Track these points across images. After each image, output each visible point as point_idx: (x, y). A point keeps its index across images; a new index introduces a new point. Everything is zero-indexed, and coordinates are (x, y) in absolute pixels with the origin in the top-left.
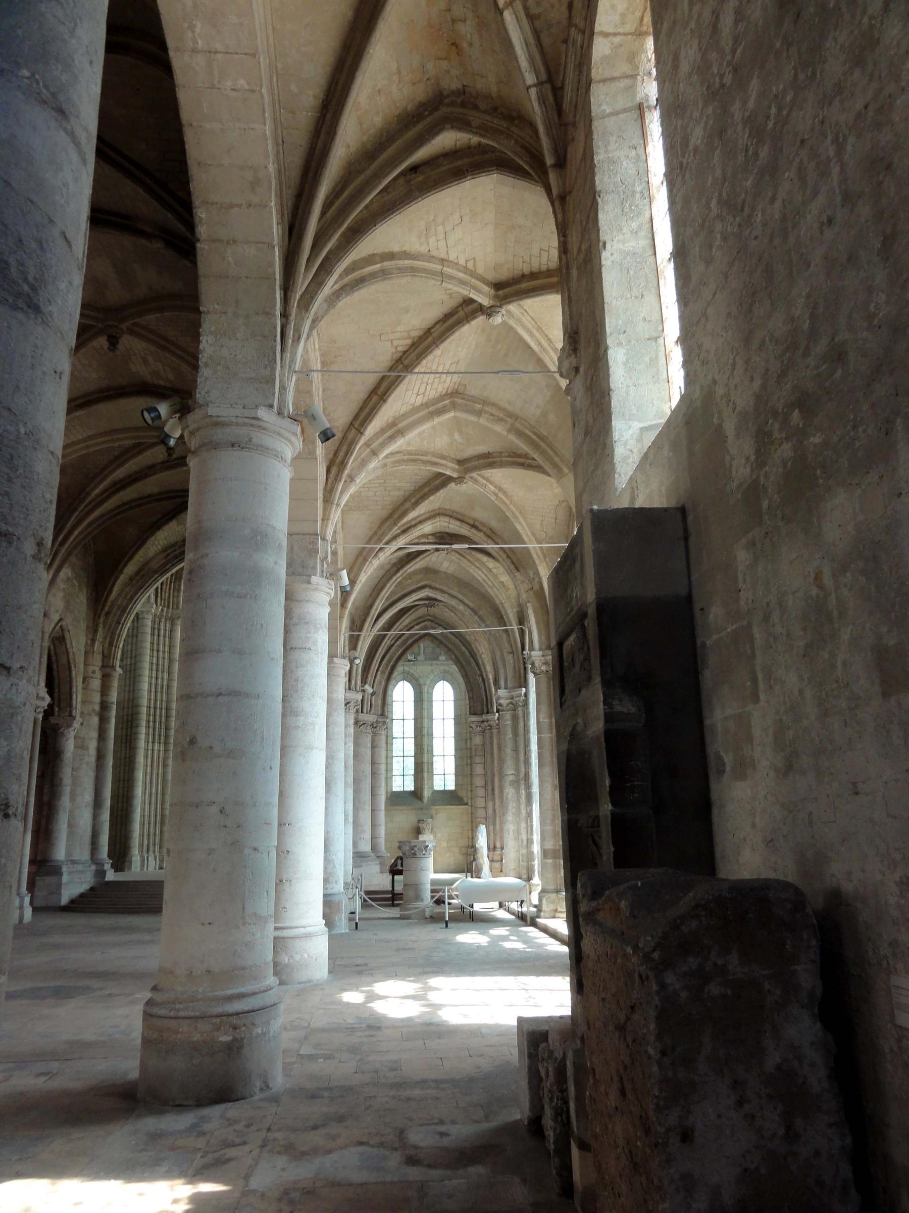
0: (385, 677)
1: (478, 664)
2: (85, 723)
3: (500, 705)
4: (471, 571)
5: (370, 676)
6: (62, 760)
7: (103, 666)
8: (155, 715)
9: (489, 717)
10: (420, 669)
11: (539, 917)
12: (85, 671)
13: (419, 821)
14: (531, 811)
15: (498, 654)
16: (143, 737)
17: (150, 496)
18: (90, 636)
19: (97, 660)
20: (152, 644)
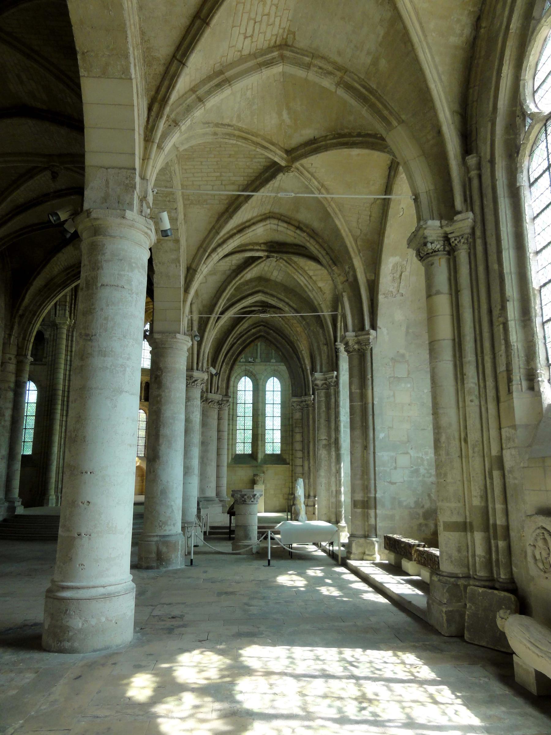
1: (298, 358)
3: (317, 385)
4: (295, 277)
9: (307, 398)
10: (258, 368)
11: (349, 559)
13: (255, 475)
14: (340, 468)
15: (315, 345)
16: (59, 411)
19: (13, 350)
20: (67, 346)
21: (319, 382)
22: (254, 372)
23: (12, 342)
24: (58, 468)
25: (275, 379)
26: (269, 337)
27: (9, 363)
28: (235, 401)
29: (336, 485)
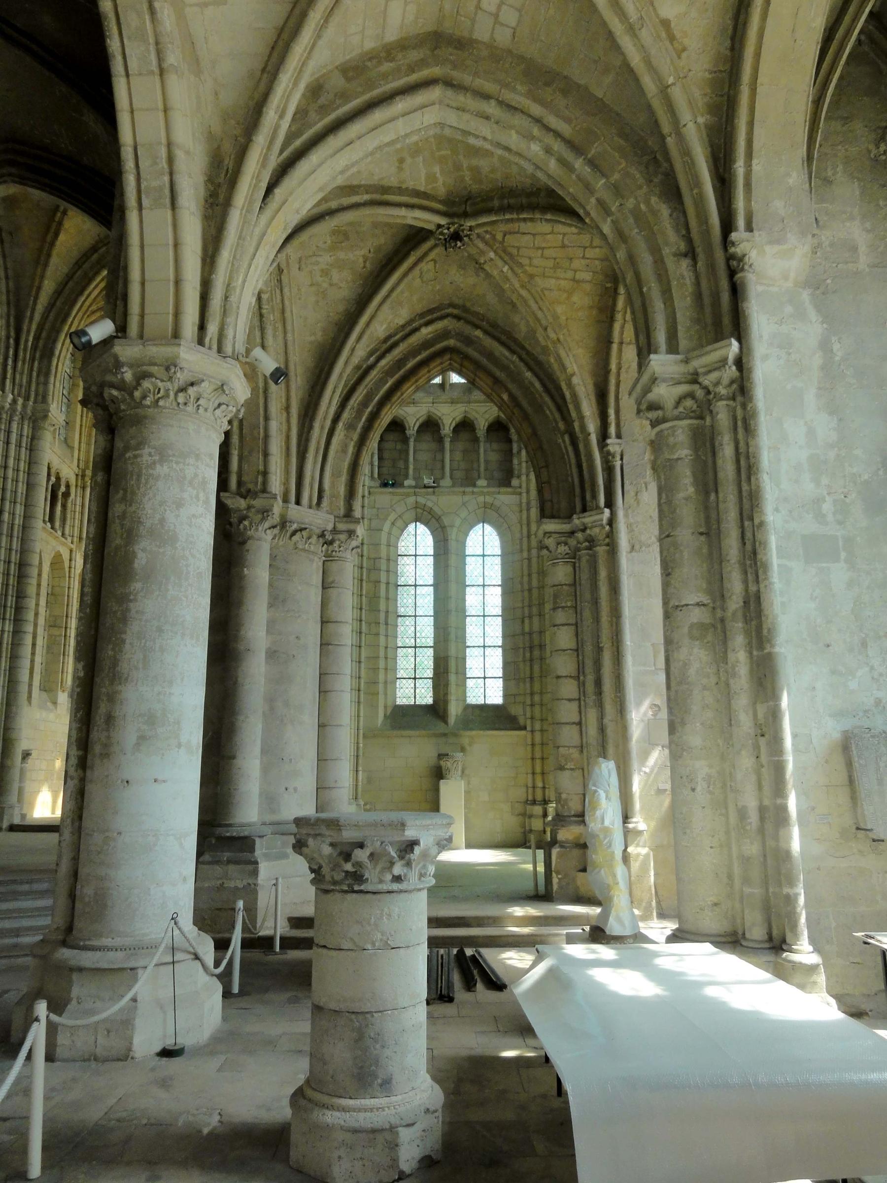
0: (355, 437)
5: (317, 425)
9: (589, 519)
10: (446, 501)
13: (441, 756)
14: (775, 715)
21: (665, 393)
22: (436, 509)
25: (488, 528)
26: (470, 351)
28: (392, 580)
29: (760, 787)
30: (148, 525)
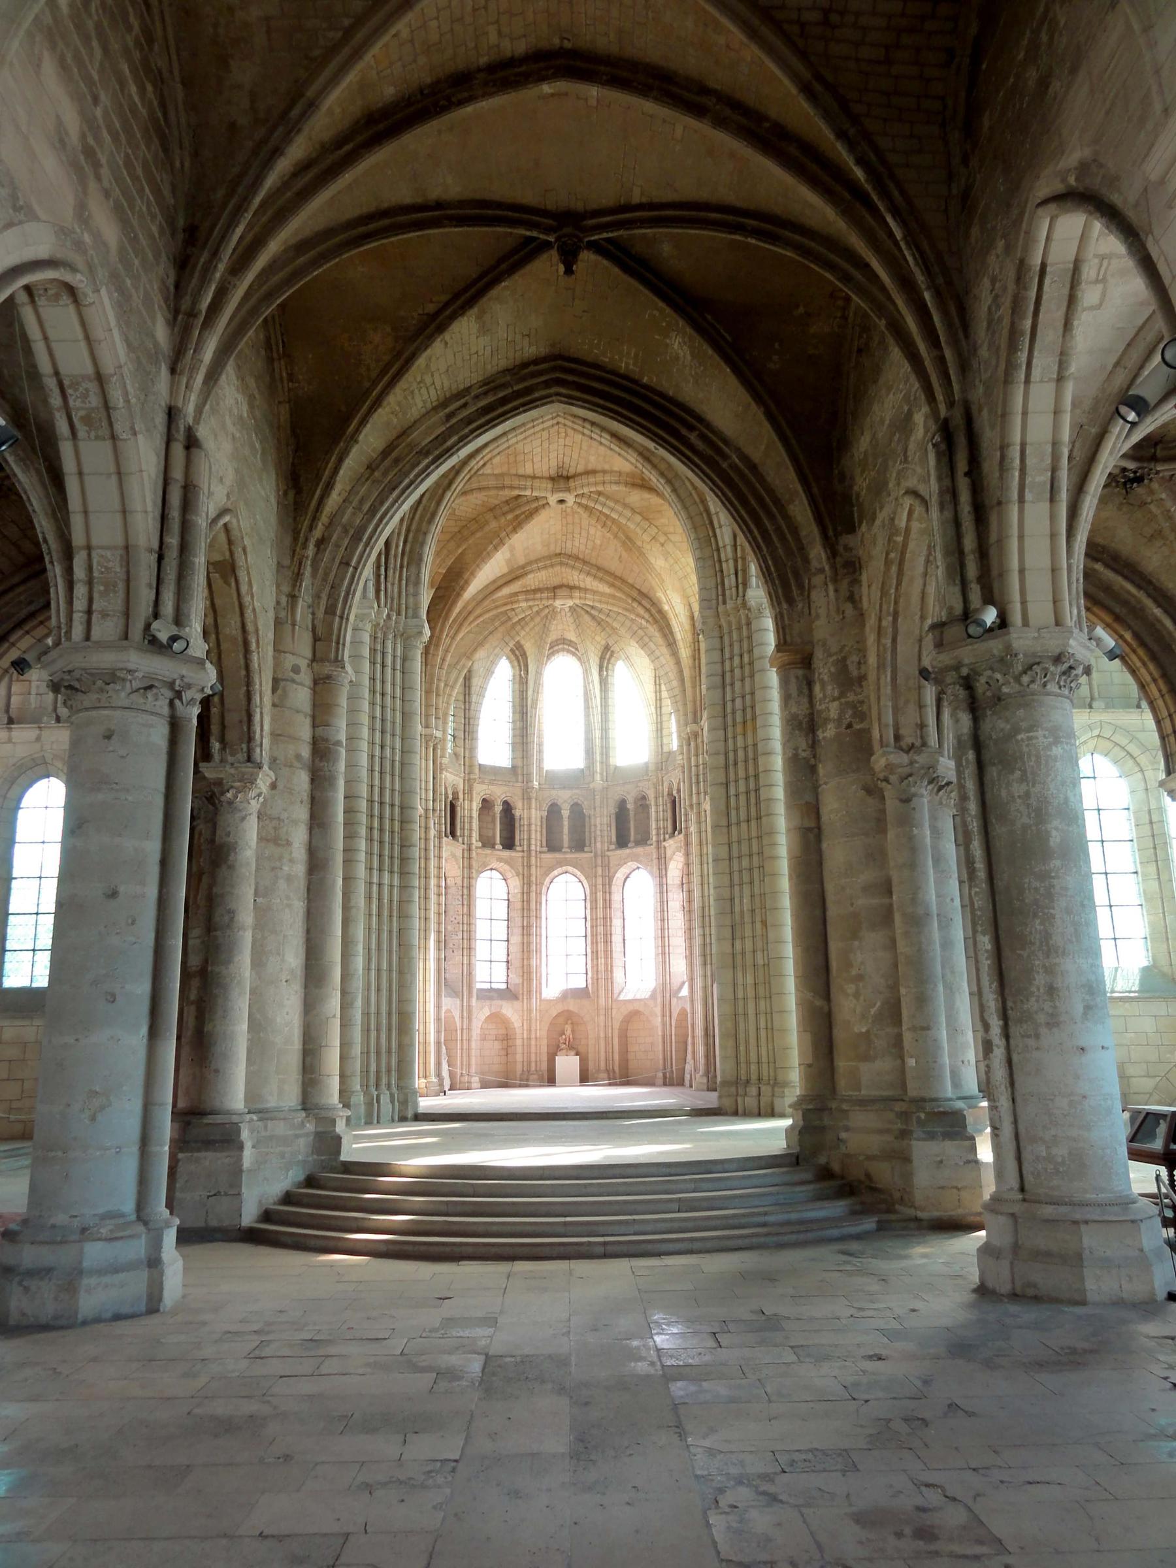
2: (280, 785)
6: (231, 867)
7: (314, 659)
8: (381, 818)
12: (277, 665)
17: (439, 205)
18: (286, 588)
19: (303, 645)
20: (373, 679)
23: (298, 617)
24: (366, 1014)
27: (293, 681)
30: (1055, 804)
